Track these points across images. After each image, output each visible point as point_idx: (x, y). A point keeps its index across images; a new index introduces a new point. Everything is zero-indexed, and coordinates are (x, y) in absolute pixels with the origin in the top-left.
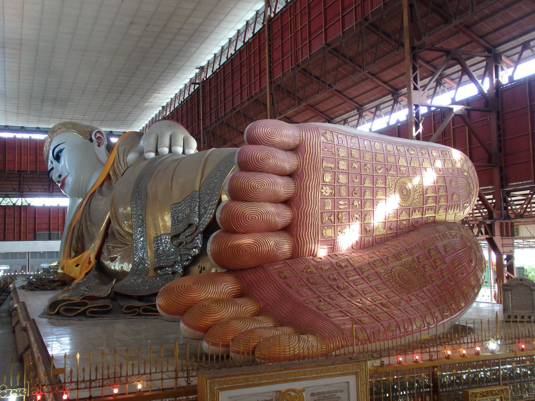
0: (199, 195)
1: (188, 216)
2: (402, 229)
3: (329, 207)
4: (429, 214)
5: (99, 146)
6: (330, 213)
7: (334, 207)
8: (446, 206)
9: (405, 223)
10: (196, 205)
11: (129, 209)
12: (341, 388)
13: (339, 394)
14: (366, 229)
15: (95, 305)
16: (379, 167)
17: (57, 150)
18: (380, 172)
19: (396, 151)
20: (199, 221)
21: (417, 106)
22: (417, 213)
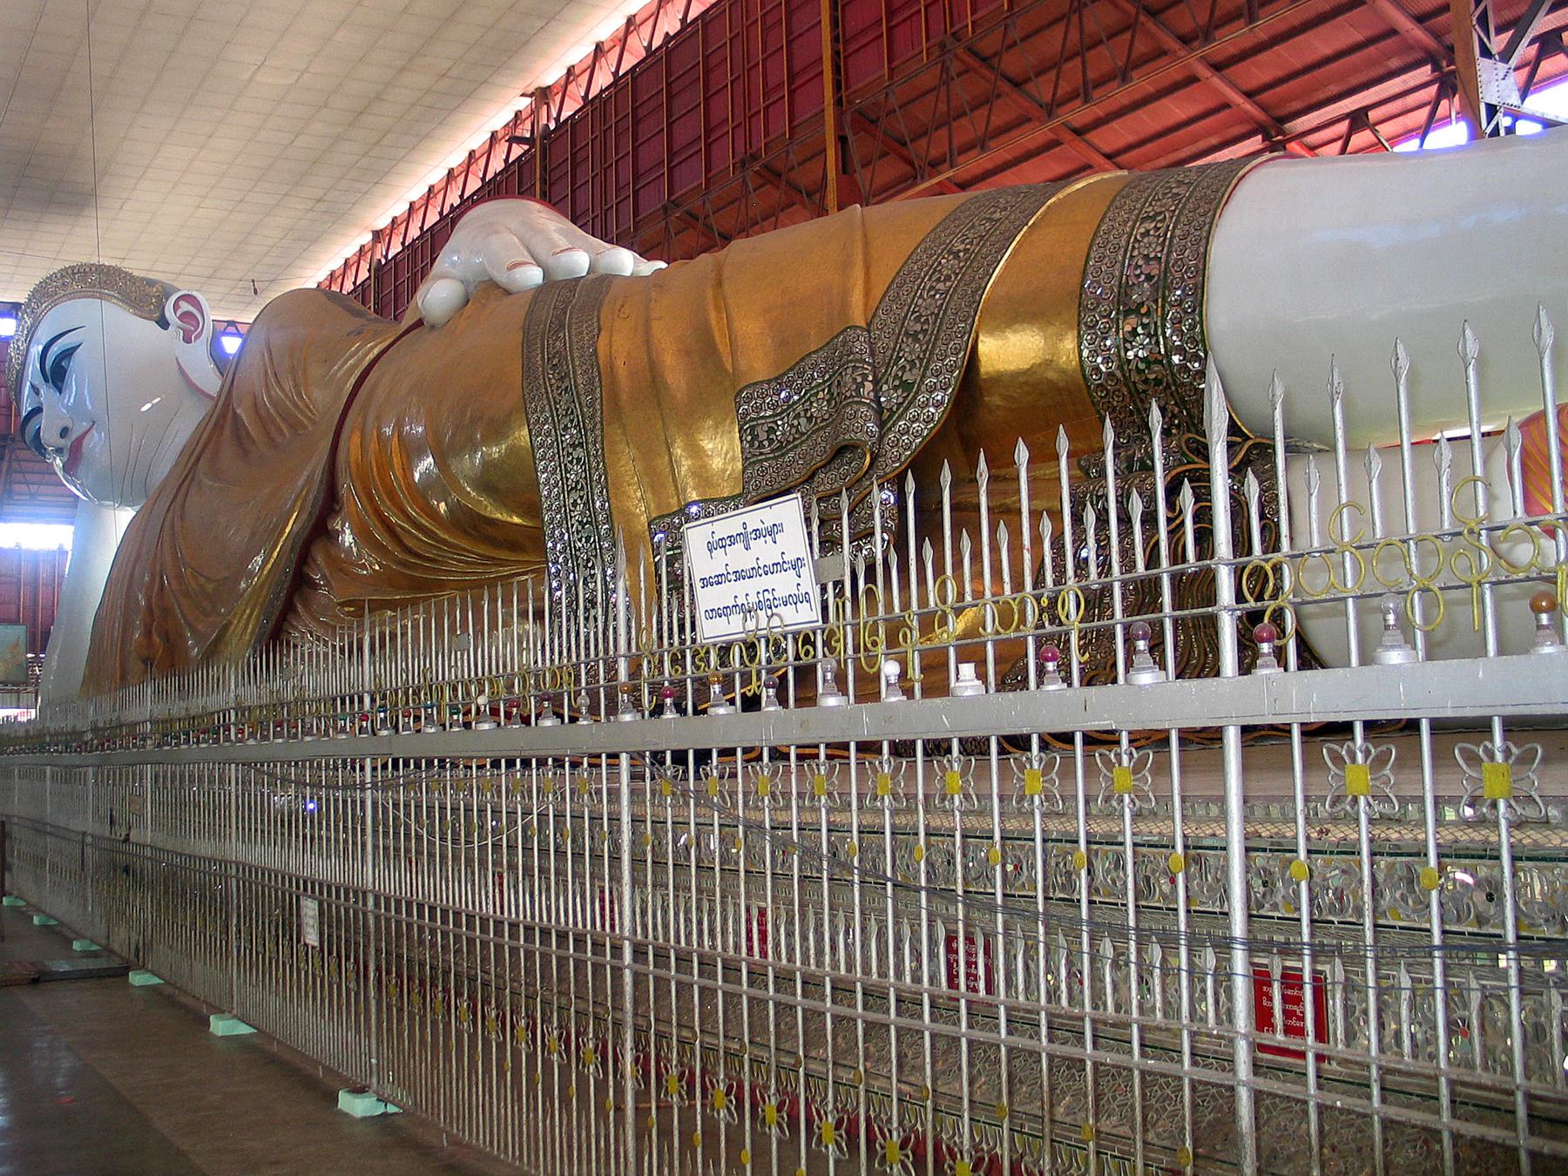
10: (865, 377)
17: (55, 349)
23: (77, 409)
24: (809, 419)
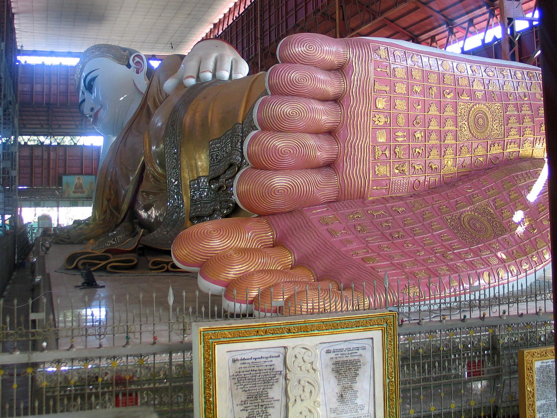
0: (242, 129)
1: (230, 154)
2: (477, 166)
3: (382, 139)
4: (512, 149)
5: (138, 72)
6: (385, 147)
7: (389, 139)
8: (532, 139)
9: (481, 159)
10: (238, 140)
11: (162, 146)
12: (364, 345)
13: (360, 352)
14: (431, 166)
15: (119, 259)
16: (448, 91)
18: (449, 97)
19: (470, 72)
20: (242, 161)
21: (511, 20)
22: (497, 147)
23: (96, 100)
24: (226, 152)
